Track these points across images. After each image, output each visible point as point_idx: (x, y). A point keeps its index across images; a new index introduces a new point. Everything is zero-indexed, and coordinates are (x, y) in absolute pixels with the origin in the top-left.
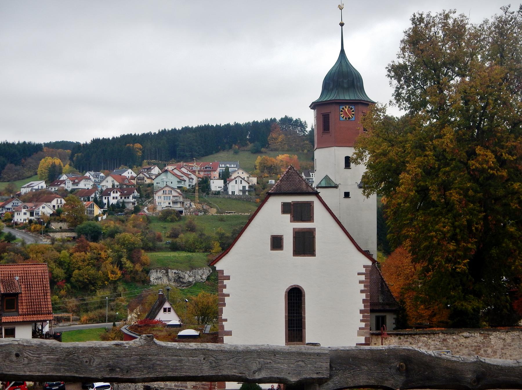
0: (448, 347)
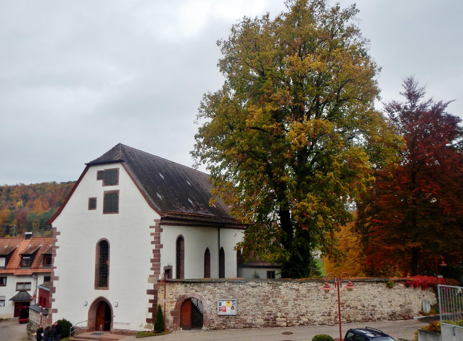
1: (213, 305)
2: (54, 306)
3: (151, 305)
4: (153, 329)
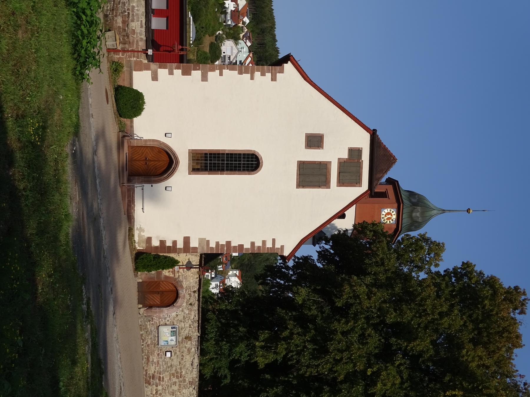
2: (163, 72)
3: (169, 244)
4: (138, 248)
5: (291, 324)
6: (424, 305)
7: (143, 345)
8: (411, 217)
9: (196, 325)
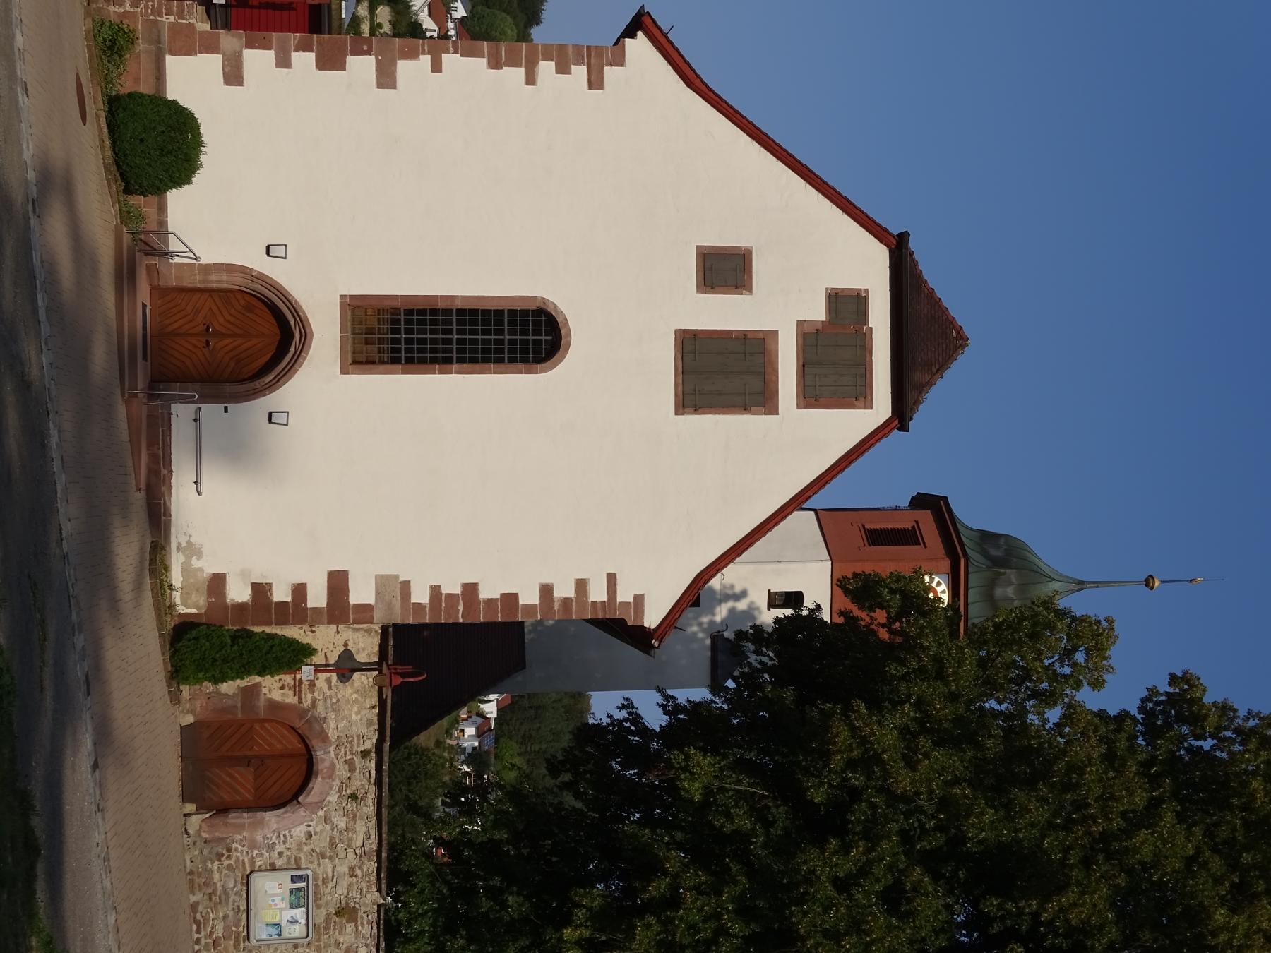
0: (326, 928)
1: (286, 853)
2: (258, 61)
3: (281, 594)
4: (183, 610)
5: (675, 859)
6: (1078, 786)
7: (198, 941)
8: (989, 598)
9: (372, 866)
